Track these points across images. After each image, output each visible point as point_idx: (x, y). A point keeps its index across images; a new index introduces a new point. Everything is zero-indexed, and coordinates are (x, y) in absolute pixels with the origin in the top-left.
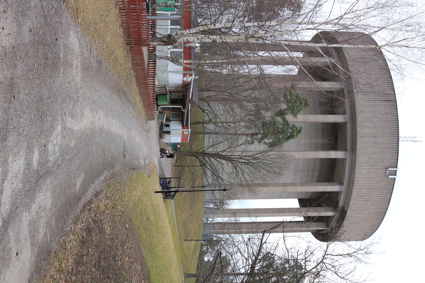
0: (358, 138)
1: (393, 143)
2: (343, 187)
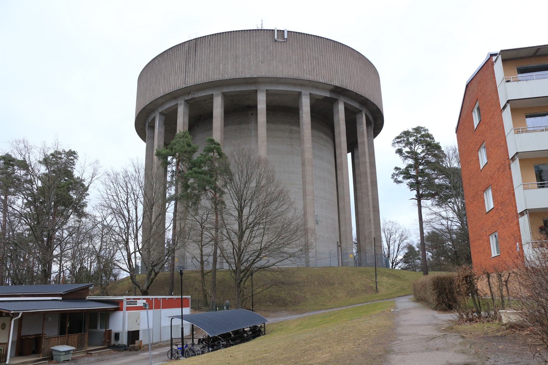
0: (238, 77)
1: (244, 36)
2: (303, 92)
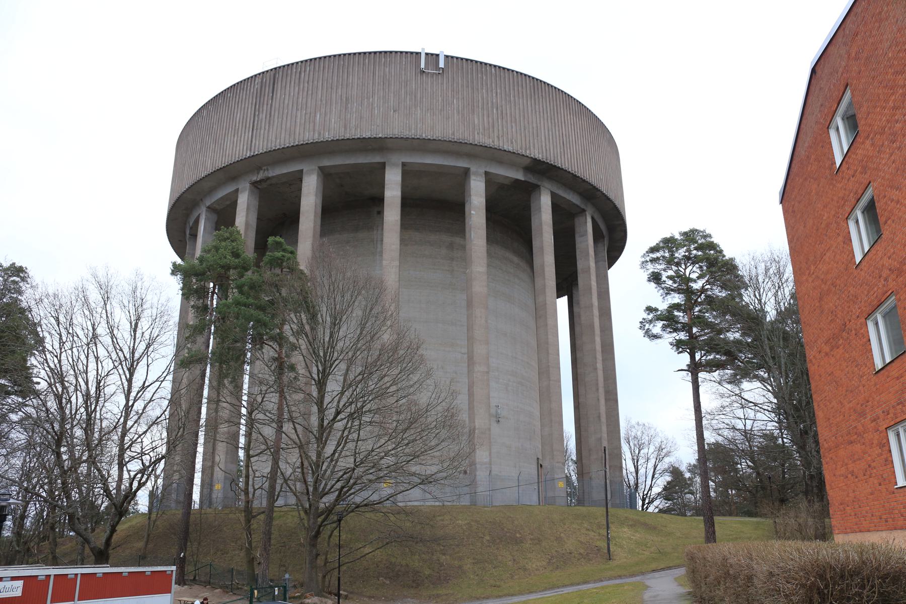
0: (348, 136)
